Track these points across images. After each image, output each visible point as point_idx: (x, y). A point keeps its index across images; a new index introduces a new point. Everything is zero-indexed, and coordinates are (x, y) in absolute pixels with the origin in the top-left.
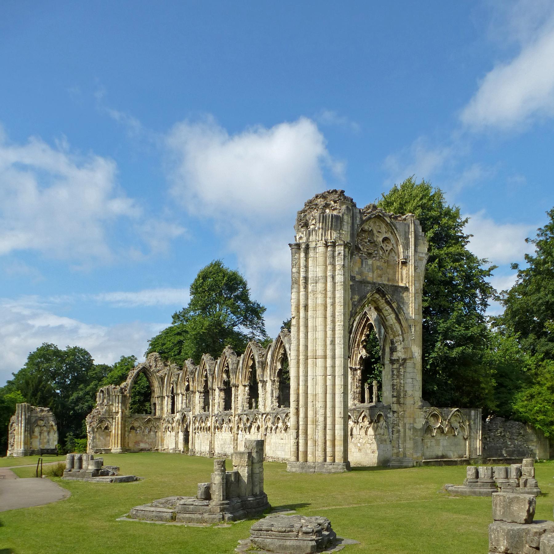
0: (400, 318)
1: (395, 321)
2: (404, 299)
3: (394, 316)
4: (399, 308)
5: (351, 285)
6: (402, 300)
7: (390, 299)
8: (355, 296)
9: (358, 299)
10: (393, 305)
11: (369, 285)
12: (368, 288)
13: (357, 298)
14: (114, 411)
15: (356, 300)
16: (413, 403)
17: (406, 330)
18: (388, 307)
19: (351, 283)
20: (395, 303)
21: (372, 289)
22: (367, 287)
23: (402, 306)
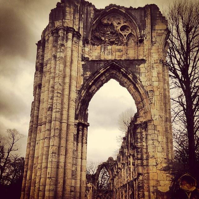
0: (137, 86)
1: (134, 90)
2: (140, 70)
3: (133, 86)
4: (135, 77)
5: (83, 65)
6: (138, 71)
7: (125, 72)
8: (87, 73)
9: (90, 75)
10: (129, 76)
11: (102, 63)
12: (101, 65)
13: (88, 74)
14: (89, 187)
15: (88, 75)
16: (155, 164)
17: (144, 96)
18: (126, 80)
19: (83, 63)
20: (130, 75)
21: (105, 65)
22: (100, 64)
23: (138, 76)
